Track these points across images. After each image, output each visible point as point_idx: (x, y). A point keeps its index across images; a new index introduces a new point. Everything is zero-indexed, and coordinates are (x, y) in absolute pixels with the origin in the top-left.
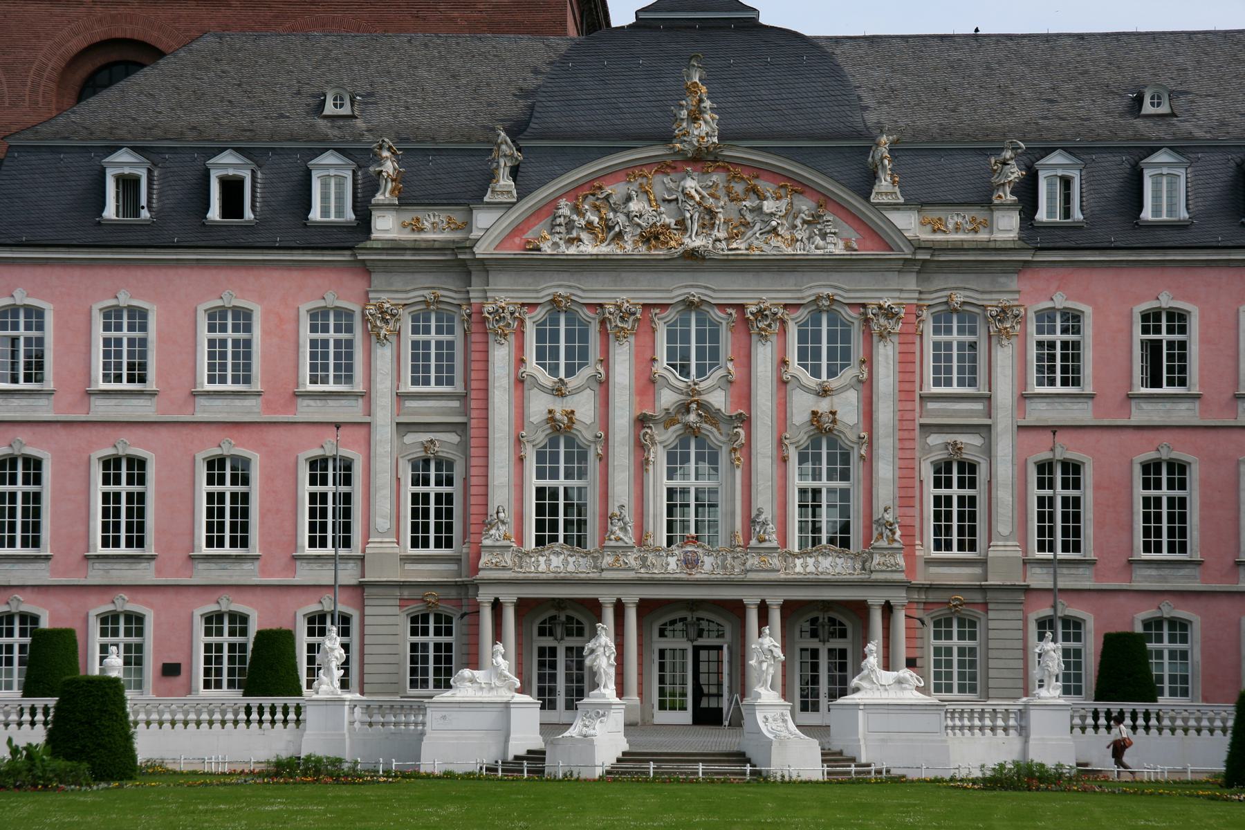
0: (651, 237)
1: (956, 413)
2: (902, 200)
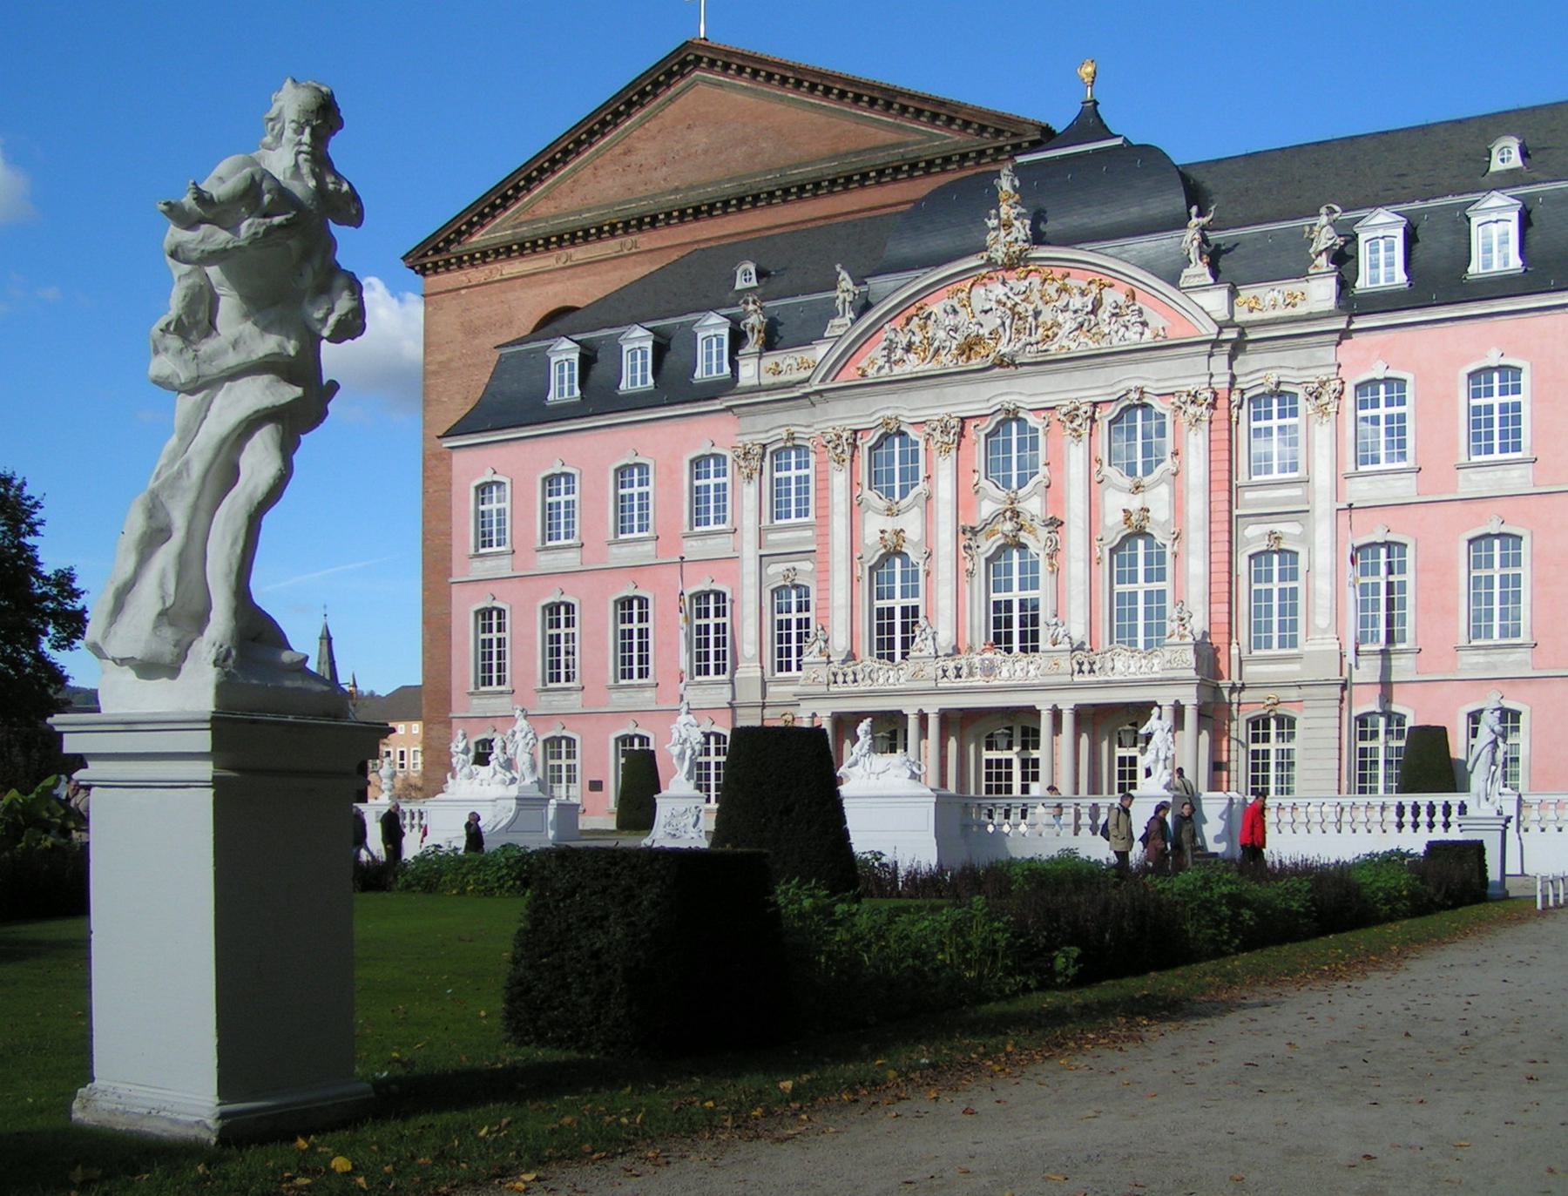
0: (969, 347)
1: (1274, 502)
2: (1211, 281)
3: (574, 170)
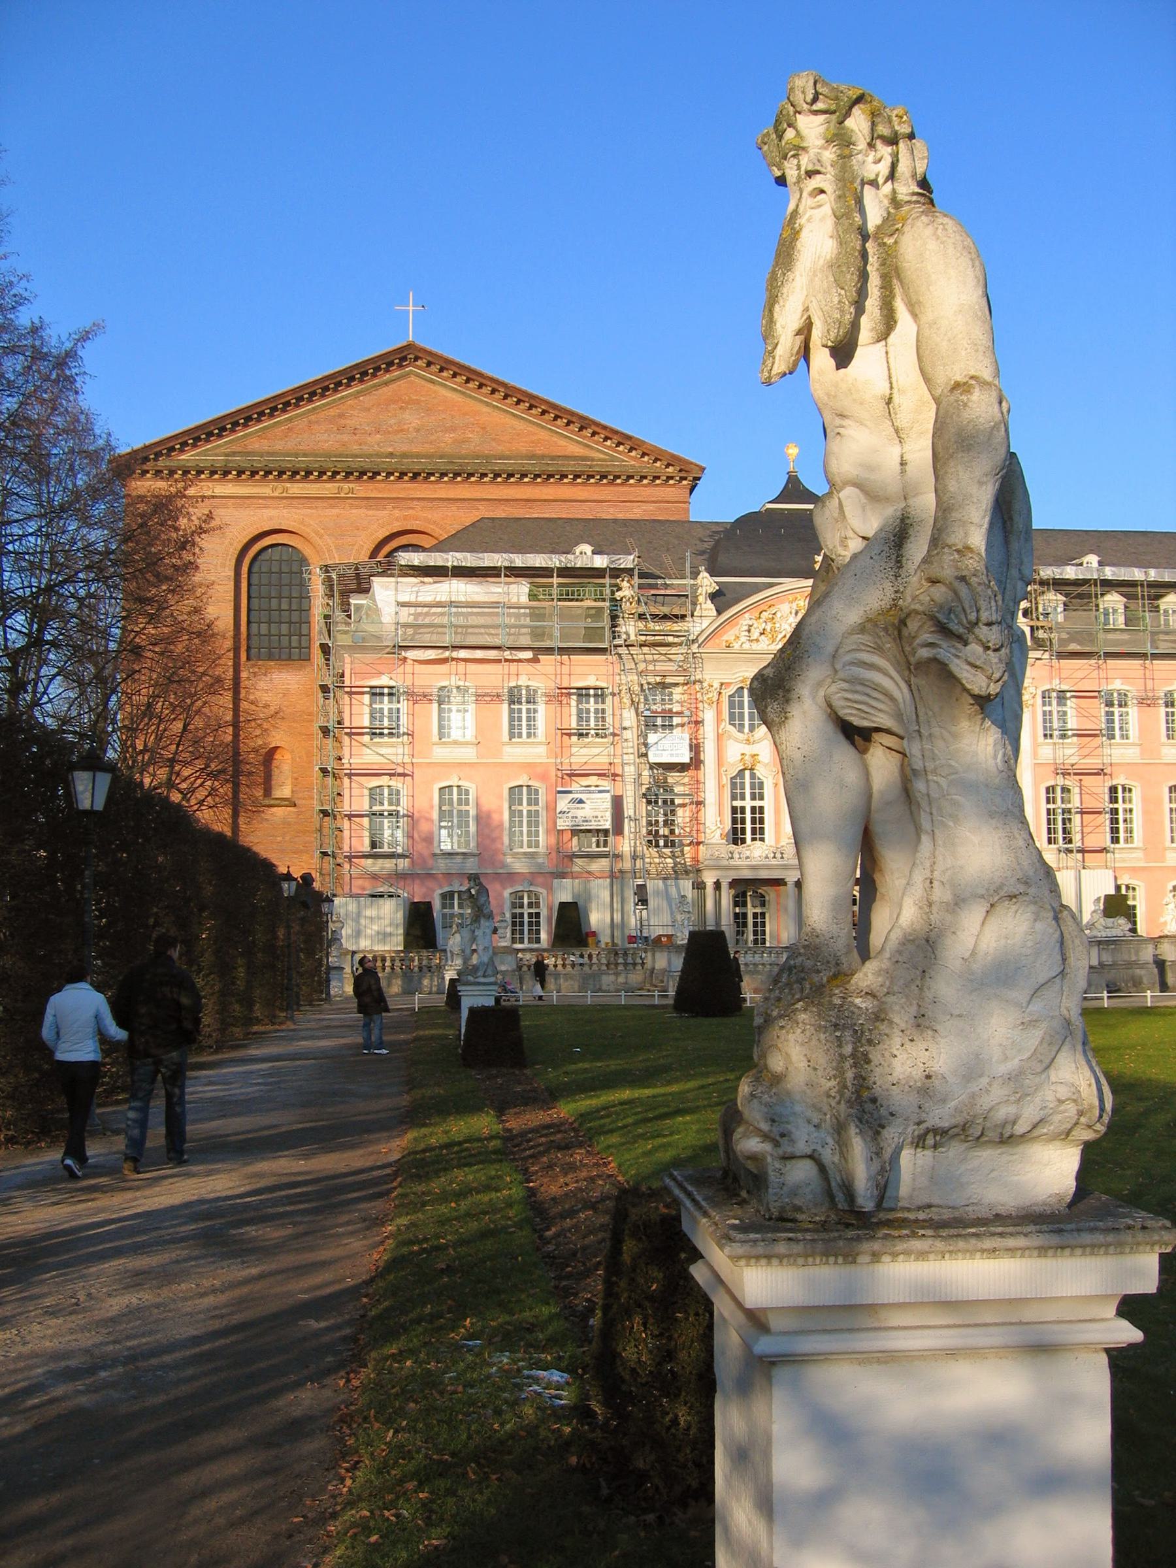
3: (290, 420)
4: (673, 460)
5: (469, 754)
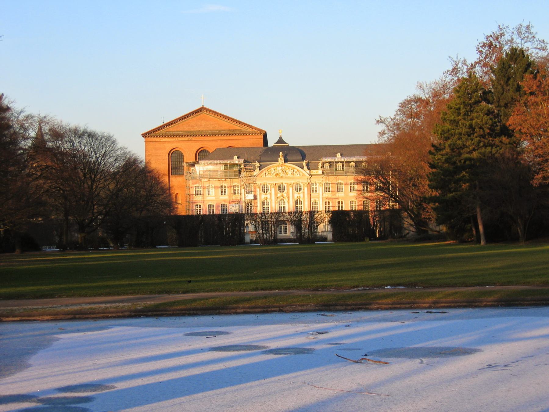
0: (277, 175)
4: (259, 130)
5: (213, 198)
